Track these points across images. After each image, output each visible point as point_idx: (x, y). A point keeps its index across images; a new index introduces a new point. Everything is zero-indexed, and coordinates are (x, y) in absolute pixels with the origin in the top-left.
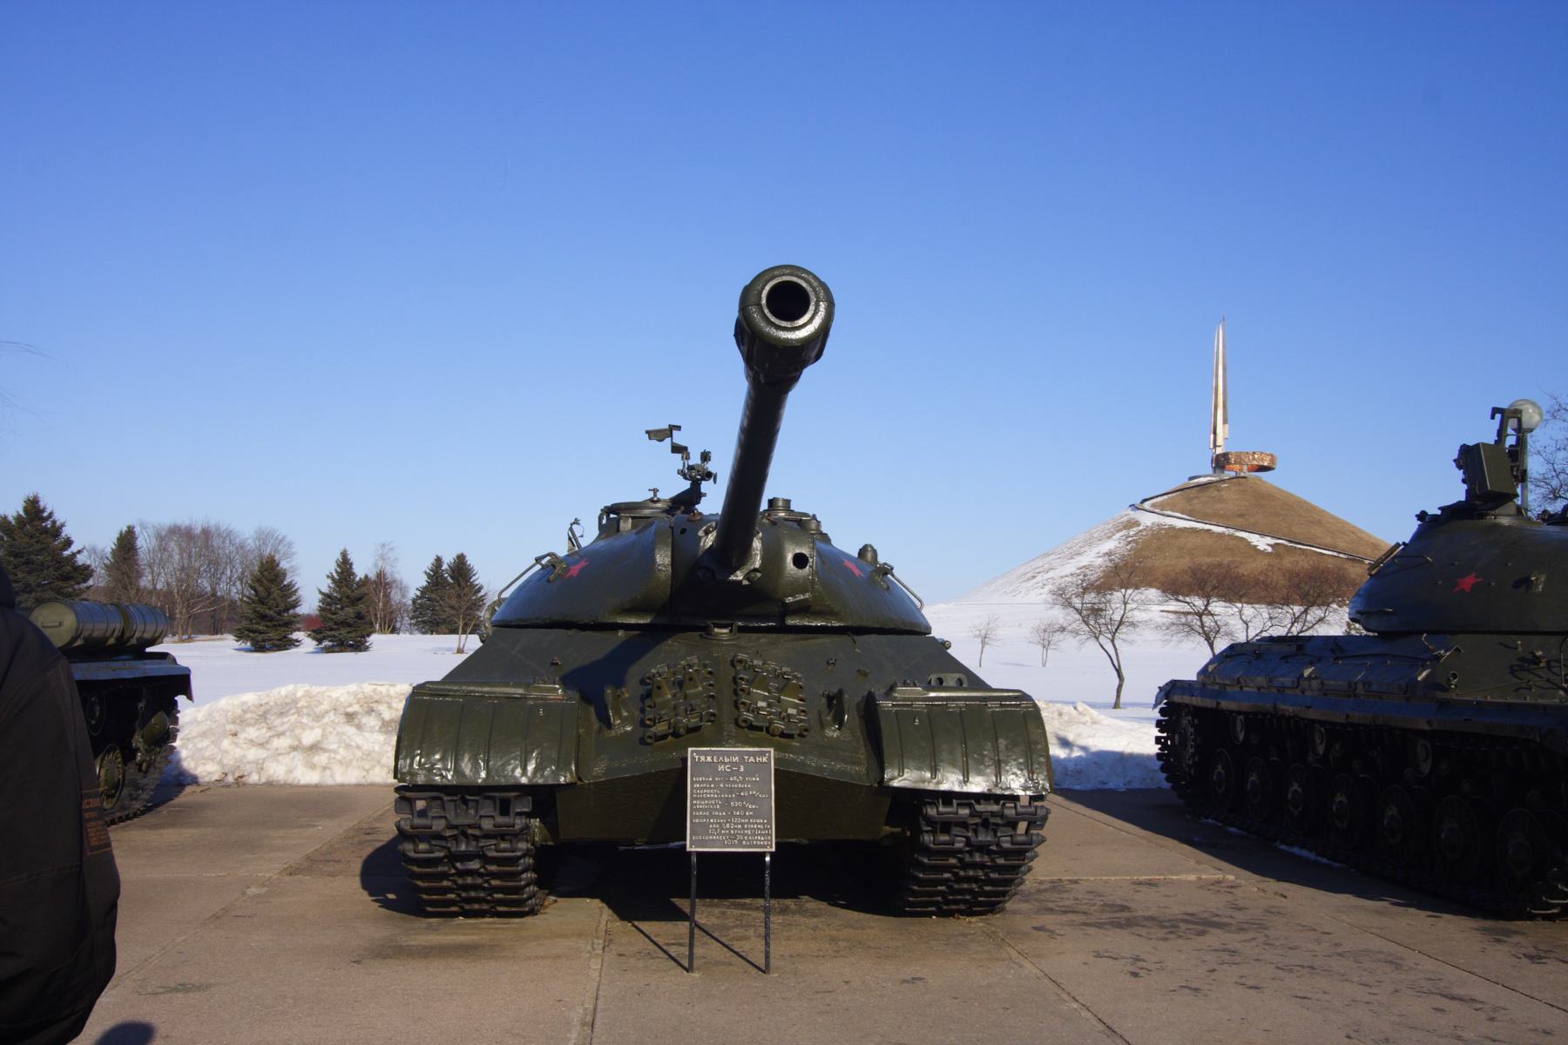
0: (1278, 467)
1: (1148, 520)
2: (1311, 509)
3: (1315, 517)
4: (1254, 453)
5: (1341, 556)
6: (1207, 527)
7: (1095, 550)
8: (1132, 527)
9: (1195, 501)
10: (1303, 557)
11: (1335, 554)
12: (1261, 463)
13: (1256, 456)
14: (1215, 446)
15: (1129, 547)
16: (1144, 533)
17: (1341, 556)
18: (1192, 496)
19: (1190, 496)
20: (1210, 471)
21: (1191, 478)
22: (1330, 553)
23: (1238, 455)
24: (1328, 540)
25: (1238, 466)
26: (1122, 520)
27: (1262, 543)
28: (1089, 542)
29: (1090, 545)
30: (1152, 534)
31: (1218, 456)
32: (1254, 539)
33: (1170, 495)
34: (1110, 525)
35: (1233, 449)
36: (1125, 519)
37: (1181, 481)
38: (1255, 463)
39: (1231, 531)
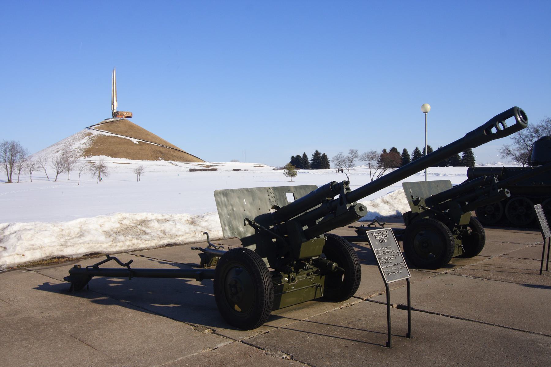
0: (133, 117)
1: (96, 133)
2: (145, 131)
3: (148, 134)
4: (126, 112)
5: (158, 145)
6: (117, 135)
7: (80, 142)
8: (90, 135)
9: (110, 127)
10: (148, 145)
11: (157, 145)
12: (129, 115)
13: (127, 113)
14: (113, 109)
15: (91, 142)
16: (95, 137)
17: (158, 145)
18: (109, 125)
19: (106, 125)
20: (112, 117)
21: (106, 120)
22: (155, 144)
23: (121, 112)
24: (153, 140)
25: (120, 116)
26: (85, 133)
27: (135, 141)
28: (75, 140)
29: (76, 141)
30: (98, 137)
31: (114, 112)
32: (132, 140)
33: (101, 125)
34: (81, 134)
35: (120, 111)
36: (86, 132)
37: (102, 120)
38: (127, 115)
39: (125, 137)
